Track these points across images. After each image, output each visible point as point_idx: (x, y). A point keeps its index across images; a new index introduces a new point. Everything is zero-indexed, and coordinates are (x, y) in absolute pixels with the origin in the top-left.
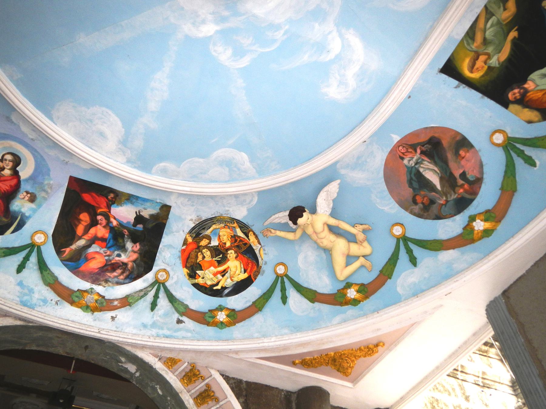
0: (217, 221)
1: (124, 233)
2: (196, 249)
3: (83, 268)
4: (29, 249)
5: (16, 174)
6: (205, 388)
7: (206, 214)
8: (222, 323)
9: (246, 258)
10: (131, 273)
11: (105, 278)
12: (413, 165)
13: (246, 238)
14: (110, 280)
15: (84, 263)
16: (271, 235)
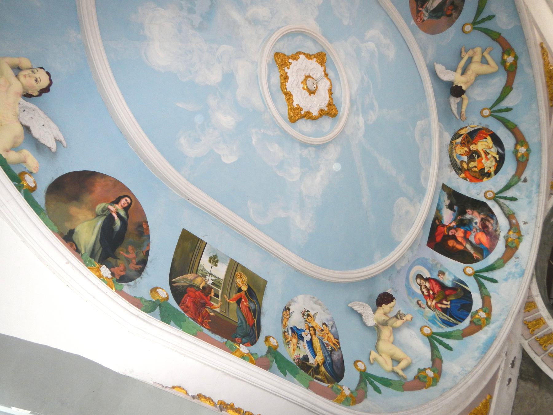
0: (451, 154)
1: (460, 218)
5: (427, 280)
8: (527, 150)
10: (488, 215)
11: (494, 232)
12: (428, 14)
13: (462, 136)
14: (495, 229)
15: (483, 245)
16: (465, 115)
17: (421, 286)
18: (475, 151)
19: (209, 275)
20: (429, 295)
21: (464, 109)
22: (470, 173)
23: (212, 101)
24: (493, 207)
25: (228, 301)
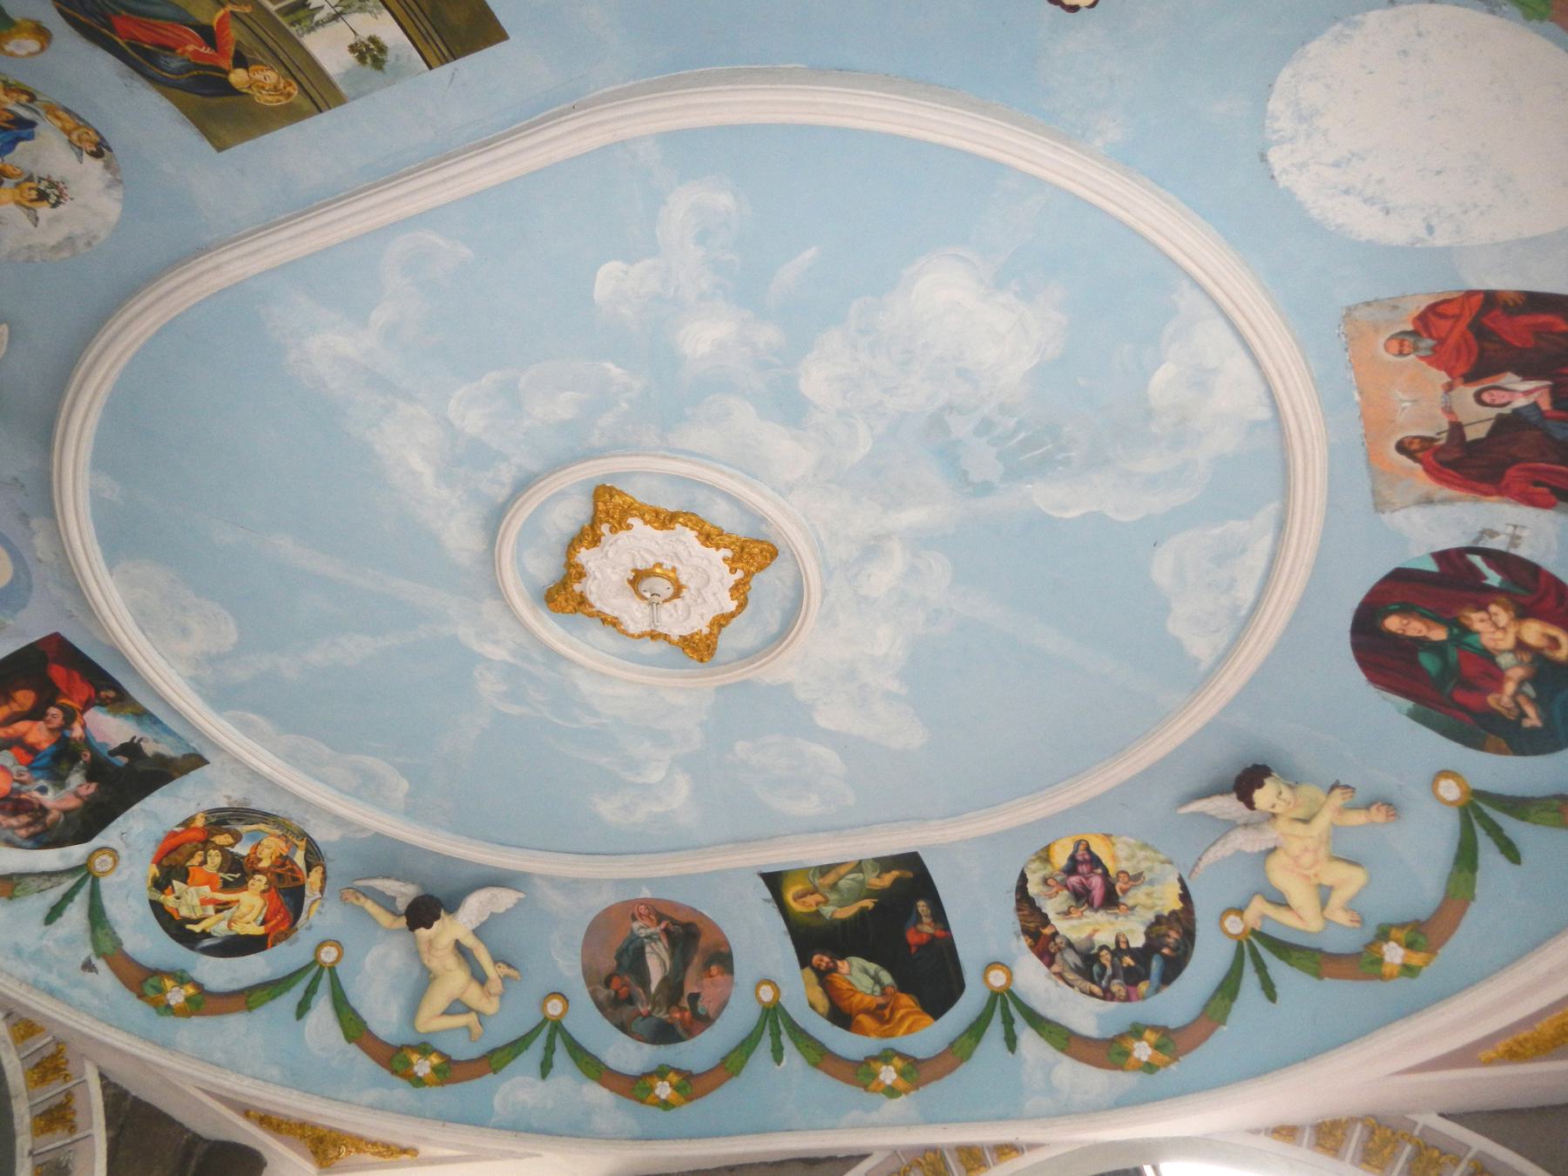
1: (83, 756)
2: (199, 842)
6: (62, 1098)
7: (257, 804)
8: (168, 1006)
10: (46, 830)
12: (643, 935)
16: (355, 902)
18: (247, 883)
19: (339, 9)
21: (370, 906)
22: (195, 843)
23: (768, 335)
24: (62, 856)
25: (230, 8)
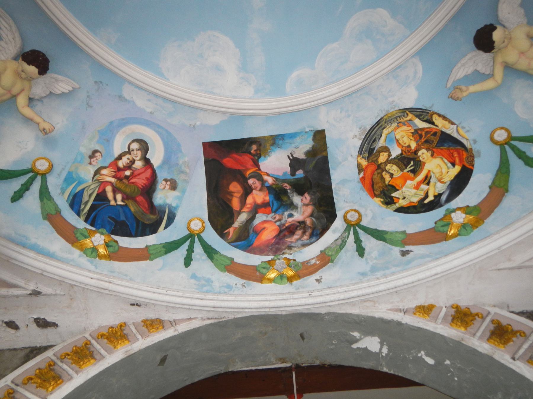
0: (385, 123)
1: (286, 188)
2: (376, 170)
3: (256, 243)
4: (189, 240)
5: (147, 162)
9: (445, 149)
10: (314, 229)
11: (286, 246)
14: (293, 245)
15: (256, 237)
17: (129, 152)
18: (420, 161)
20: (119, 169)
22: (376, 173)
